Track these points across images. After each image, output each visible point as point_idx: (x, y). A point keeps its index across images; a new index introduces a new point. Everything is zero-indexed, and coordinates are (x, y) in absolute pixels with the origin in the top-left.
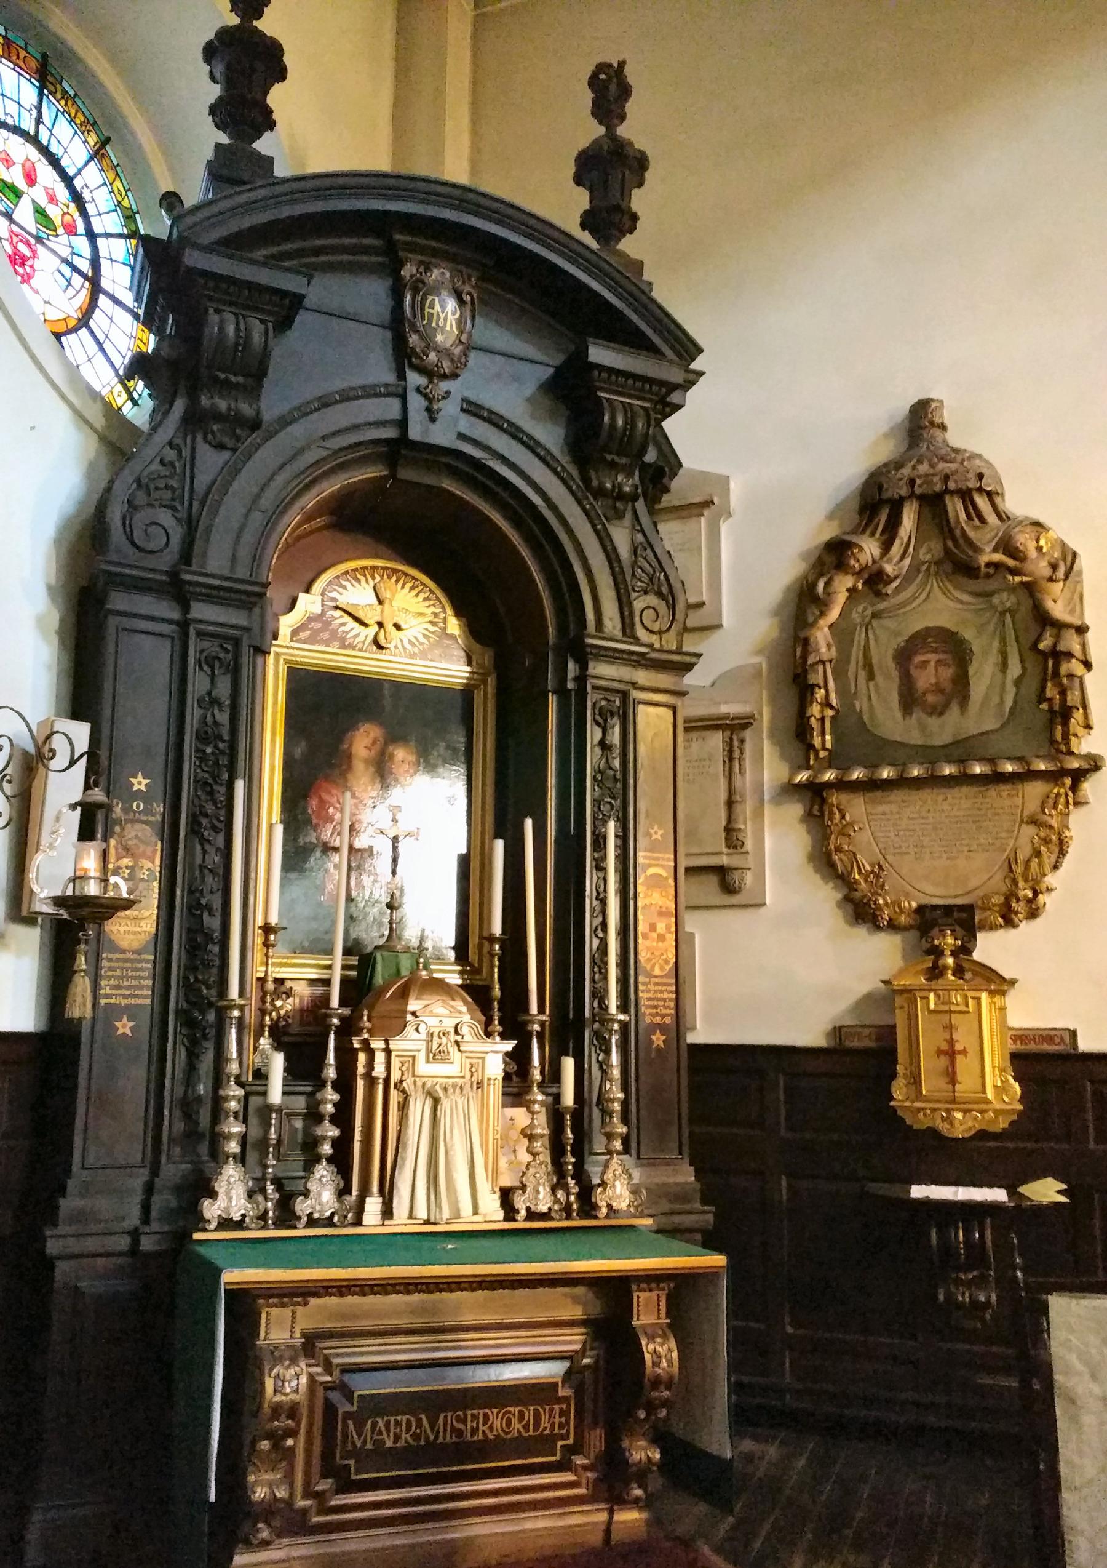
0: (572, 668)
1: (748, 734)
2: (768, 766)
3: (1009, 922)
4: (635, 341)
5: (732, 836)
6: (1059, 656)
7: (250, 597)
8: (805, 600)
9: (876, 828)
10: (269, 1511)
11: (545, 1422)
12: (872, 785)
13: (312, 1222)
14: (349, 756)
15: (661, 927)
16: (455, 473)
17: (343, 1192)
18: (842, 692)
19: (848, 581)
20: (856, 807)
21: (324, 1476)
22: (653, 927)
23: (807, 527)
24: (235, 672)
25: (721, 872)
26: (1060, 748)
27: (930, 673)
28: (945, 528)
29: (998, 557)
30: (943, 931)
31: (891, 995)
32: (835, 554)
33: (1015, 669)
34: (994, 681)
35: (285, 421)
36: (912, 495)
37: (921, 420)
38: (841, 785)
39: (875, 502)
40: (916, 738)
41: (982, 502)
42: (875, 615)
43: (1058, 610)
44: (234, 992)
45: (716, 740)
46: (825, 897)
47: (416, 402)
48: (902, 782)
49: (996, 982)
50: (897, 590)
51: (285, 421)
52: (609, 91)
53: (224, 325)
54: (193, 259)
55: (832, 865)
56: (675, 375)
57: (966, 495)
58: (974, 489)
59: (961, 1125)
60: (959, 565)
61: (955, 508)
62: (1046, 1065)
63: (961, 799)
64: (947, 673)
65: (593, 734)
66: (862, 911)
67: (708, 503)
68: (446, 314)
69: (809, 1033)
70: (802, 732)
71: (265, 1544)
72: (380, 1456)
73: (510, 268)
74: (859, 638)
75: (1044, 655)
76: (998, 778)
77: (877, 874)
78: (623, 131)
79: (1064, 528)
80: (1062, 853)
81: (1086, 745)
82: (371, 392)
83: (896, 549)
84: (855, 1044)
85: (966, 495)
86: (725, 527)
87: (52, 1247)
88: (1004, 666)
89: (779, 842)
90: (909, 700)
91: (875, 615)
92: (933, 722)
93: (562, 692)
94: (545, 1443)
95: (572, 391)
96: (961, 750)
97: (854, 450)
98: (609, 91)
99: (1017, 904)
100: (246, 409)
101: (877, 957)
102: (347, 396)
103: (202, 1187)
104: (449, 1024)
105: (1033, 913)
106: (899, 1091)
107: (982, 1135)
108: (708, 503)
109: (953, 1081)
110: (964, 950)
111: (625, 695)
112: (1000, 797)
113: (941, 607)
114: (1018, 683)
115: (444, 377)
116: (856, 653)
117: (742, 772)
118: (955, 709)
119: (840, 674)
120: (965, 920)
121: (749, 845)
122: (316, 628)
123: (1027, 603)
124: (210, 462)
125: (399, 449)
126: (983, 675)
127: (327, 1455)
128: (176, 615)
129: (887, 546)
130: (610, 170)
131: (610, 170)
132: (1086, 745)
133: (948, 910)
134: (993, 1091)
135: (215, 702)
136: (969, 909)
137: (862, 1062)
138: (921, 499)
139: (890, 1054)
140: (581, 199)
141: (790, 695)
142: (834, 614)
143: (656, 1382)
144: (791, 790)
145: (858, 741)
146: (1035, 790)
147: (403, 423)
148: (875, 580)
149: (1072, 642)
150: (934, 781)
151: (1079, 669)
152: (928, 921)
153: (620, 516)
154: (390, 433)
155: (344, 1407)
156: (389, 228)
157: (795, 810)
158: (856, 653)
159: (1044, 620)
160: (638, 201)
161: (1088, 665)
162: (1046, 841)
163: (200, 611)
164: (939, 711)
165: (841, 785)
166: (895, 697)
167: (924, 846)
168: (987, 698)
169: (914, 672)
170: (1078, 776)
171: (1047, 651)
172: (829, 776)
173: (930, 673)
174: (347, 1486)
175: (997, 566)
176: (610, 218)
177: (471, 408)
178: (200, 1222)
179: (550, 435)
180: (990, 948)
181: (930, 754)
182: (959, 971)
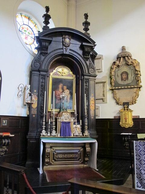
0: (82, 77)
1: (105, 83)
2: (108, 87)
3: (133, 104)
4: (88, 42)
5: (104, 95)
6: (137, 74)
7: (47, 71)
8: (111, 68)
9: (119, 93)
10: (47, 163)
11: (76, 156)
12: (118, 89)
13: (53, 136)
14: (59, 87)
15: (93, 105)
16: (69, 57)
17: (56, 133)
18: (115, 78)
19: (116, 66)
20: (117, 91)
21: (53, 160)
22: (92, 105)
24: (45, 79)
25: (102, 99)
26: (137, 84)
28: (126, 61)
29: (131, 63)
30: (126, 105)
31: (120, 112)
32: (114, 63)
33: (133, 76)
34: (131, 77)
35: (50, 53)
36: (122, 57)
37: (123, 48)
38: (115, 89)
39: (118, 58)
40: (123, 84)
41: (129, 57)
42: (118, 70)
43: (137, 69)
44: (44, 113)
47: (64, 50)
49: (131, 111)
50: (121, 67)
51: (50, 53)
52: (86, 16)
53: (44, 44)
54: (40, 38)
55: (114, 98)
56: (93, 45)
57: (127, 56)
58: (129, 56)
59: (127, 126)
60: (127, 64)
61: (126, 58)
62: (136, 120)
63: (128, 90)
64: (126, 76)
65: (85, 84)
66: (118, 103)
67: (101, 58)
68: (67, 40)
69: (112, 117)
70: (111, 83)
71: (47, 166)
72: (59, 158)
73: (74, 35)
74: (117, 72)
75: (136, 74)
76: (131, 88)
77: (119, 99)
78: (87, 20)
79: (138, 60)
80: (138, 96)
81: (141, 84)
82: (60, 49)
83: (120, 63)
84: (116, 118)
85: (127, 56)
87: (27, 137)
88: (132, 76)
89: (109, 95)
90: (122, 79)
91: (118, 70)
92: (125, 82)
93: (81, 80)
94: (76, 158)
95: (82, 47)
96: (127, 85)
98: (86, 16)
99: (134, 102)
100: (46, 52)
101: (120, 108)
102: (57, 50)
103: (41, 132)
104: (67, 116)
105: (135, 103)
106: (121, 123)
107: (129, 127)
108: (101, 58)
109: (126, 121)
110: (128, 107)
111: (88, 80)
112: (132, 90)
113: (125, 69)
114: (133, 77)
115: (67, 47)
116: (117, 74)
117: (105, 88)
118: (127, 80)
119: (115, 77)
121: (105, 96)
122: (55, 74)
123: (134, 69)
124: (43, 58)
125: (63, 55)
126: (130, 76)
127: (53, 158)
128: (39, 73)
129: (120, 62)
130: (86, 24)
131: (86, 24)
132: (141, 84)
133: (126, 103)
134: (130, 123)
135: (43, 82)
136: (128, 103)
137: (117, 120)
138: (124, 57)
139: (120, 119)
140: (83, 27)
141: (110, 79)
142: (114, 70)
143: (88, 152)
145: (117, 84)
146: (135, 89)
147: (63, 52)
148: (118, 66)
149: (139, 73)
150: (125, 88)
151: (140, 76)
152: (124, 104)
153: (88, 60)
154: (62, 53)
155: (55, 153)
157: (111, 92)
158: (117, 74)
159: (136, 70)
160: (89, 27)
161: (141, 75)
162: (137, 95)
163: (41, 73)
164: (125, 81)
165: (115, 89)
166: (121, 80)
167: (124, 95)
168: (130, 79)
169: (123, 76)
170: (140, 88)
171: (137, 74)
172: (114, 88)
174: (55, 161)
175: (131, 64)
176: (86, 29)
177: (70, 50)
178: (41, 135)
179: (81, 52)
180: (131, 107)
181: (124, 85)
182: (127, 110)
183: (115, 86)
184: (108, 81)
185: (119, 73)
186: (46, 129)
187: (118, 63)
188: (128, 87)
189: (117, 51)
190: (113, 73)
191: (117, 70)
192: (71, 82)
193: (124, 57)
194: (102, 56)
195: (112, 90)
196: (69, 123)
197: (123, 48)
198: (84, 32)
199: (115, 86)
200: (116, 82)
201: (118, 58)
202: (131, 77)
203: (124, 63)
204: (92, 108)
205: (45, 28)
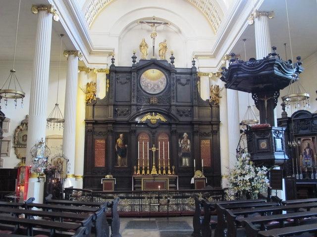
2: (12, 144)
5: (8, 151)
8: (16, 131)
20: (18, 149)
23: (17, 123)
31: (19, 164)
32: (18, 127)
39: (22, 124)
45: (7, 142)
46: (15, 156)
66: (18, 157)
86: (10, 123)
90: (23, 140)
101: (19, 161)
145: (19, 144)
148: (21, 130)
157: (13, 149)
183: (17, 145)
184: (12, 140)
185: (22, 135)
187: (21, 127)
189: (22, 118)
190: (17, 135)
194: (10, 119)
195: (15, 147)
199: (17, 145)
200: (18, 142)
201: (22, 124)
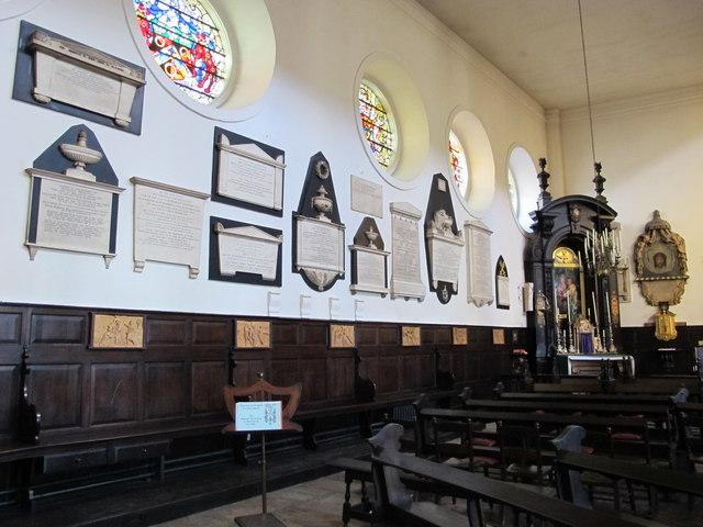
8: (636, 247)
9: (651, 288)
20: (647, 284)
27: (659, 261)
30: (663, 306)
31: (654, 317)
32: (641, 238)
34: (671, 262)
35: (556, 232)
37: (656, 214)
39: (648, 230)
46: (643, 300)
48: (655, 280)
49: (673, 315)
52: (598, 167)
53: (547, 222)
58: (666, 228)
59: (667, 338)
60: (664, 242)
63: (666, 283)
66: (649, 303)
68: (576, 212)
69: (641, 325)
70: (637, 271)
73: (584, 202)
77: (651, 297)
81: (687, 274)
90: (656, 266)
96: (666, 275)
97: (646, 219)
98: (598, 167)
99: (676, 301)
101: (653, 310)
112: (672, 282)
113: (661, 249)
120: (667, 304)
124: (545, 241)
126: (668, 261)
131: (600, 181)
132: (687, 274)
134: (672, 332)
137: (649, 330)
138: (656, 230)
144: (635, 281)
145: (647, 273)
148: (649, 244)
150: (660, 280)
156: (570, 203)
167: (659, 291)
170: (685, 279)
171: (680, 258)
173: (659, 261)
176: (600, 190)
180: (671, 309)
181: (661, 275)
183: (644, 276)
184: (631, 267)
185: (651, 255)
186: (562, 344)
187: (647, 238)
188: (664, 277)
190: (640, 255)
191: (646, 249)
192: (577, 271)
193: (656, 230)
195: (640, 282)
196: (590, 334)
197: (656, 214)
198: (594, 195)
202: (671, 262)
203: (658, 239)
204: (615, 311)
205: (546, 195)
